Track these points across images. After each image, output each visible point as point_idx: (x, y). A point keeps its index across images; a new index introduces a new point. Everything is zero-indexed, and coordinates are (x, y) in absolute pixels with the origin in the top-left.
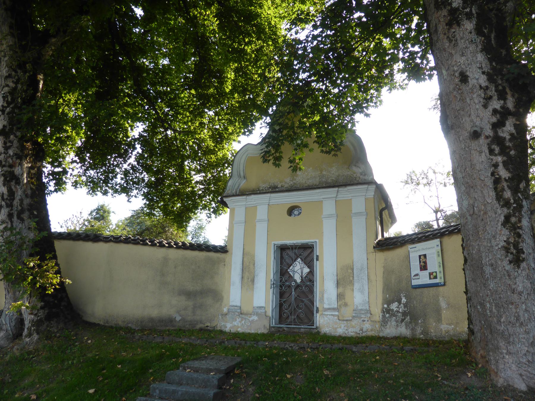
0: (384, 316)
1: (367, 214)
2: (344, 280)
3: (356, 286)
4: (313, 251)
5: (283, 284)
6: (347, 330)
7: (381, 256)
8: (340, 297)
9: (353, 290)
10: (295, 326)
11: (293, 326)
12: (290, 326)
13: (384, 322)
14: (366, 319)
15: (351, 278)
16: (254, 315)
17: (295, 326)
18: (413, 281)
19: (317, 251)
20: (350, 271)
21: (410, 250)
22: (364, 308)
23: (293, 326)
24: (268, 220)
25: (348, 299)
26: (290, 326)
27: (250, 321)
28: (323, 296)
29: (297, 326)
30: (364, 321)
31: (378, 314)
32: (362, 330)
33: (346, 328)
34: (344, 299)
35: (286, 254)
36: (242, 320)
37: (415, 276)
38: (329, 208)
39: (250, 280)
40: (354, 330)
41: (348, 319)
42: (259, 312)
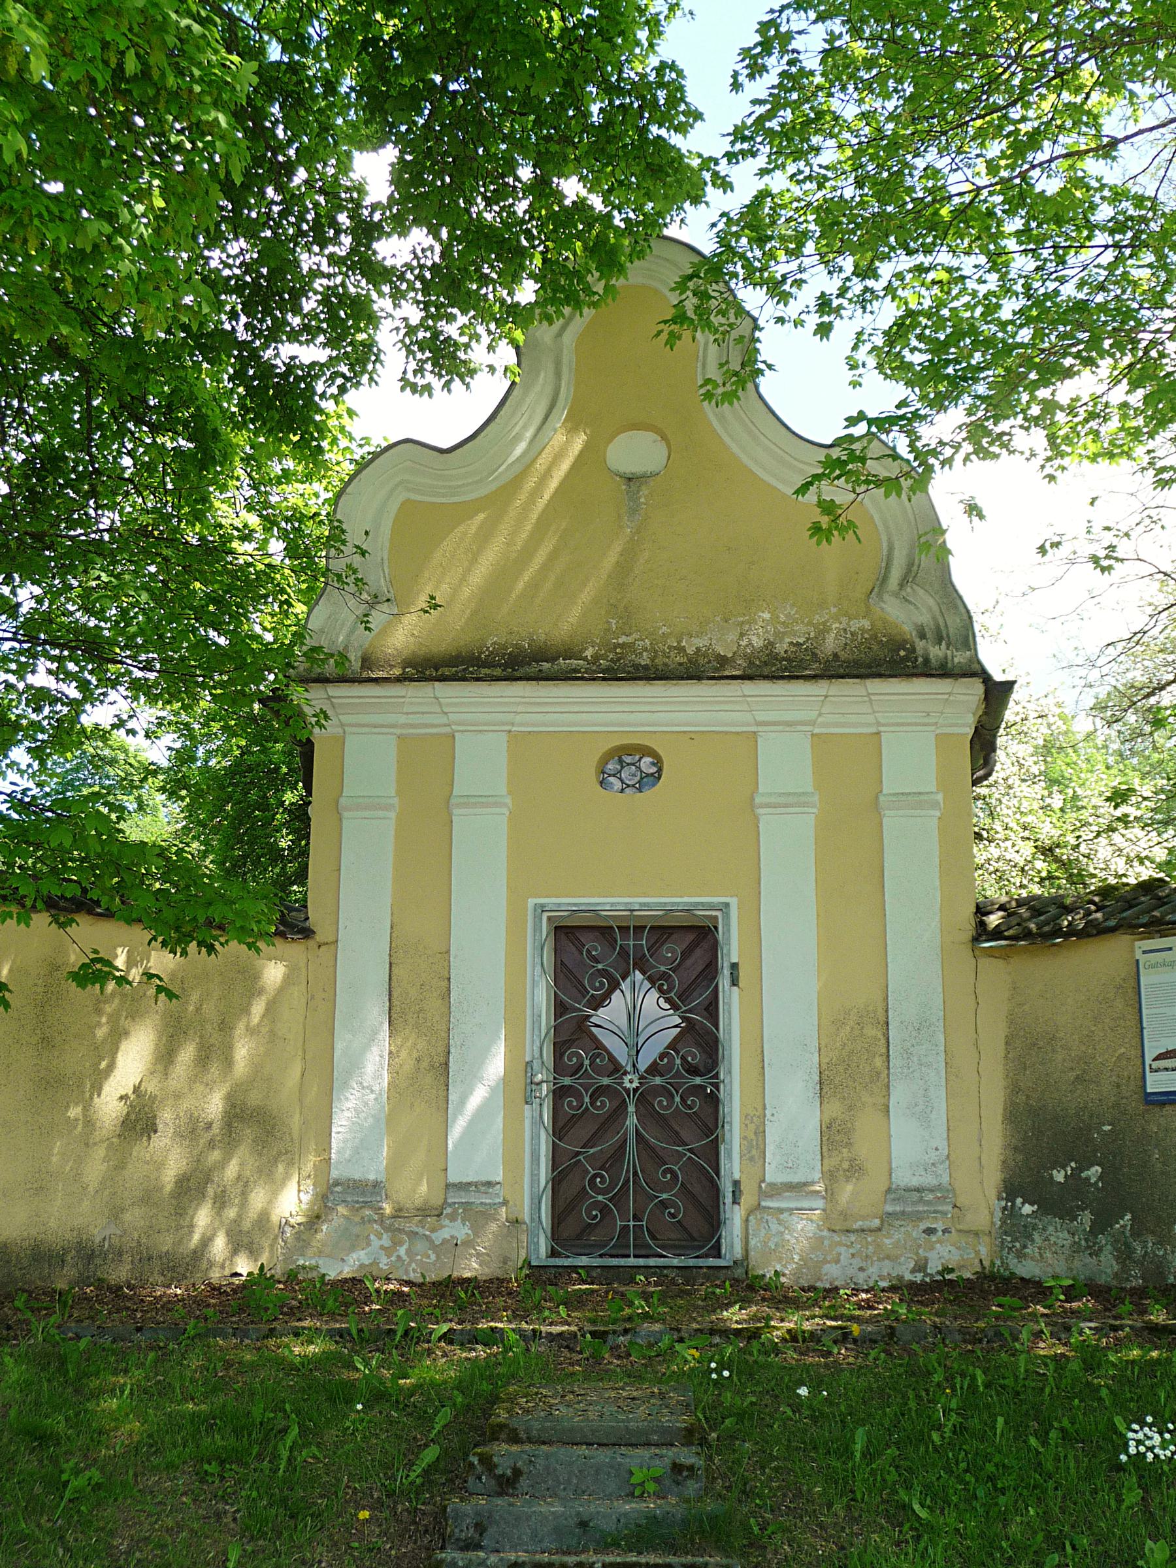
0: (1010, 1213)
1: (752, 805)
2: (854, 1071)
3: (899, 1095)
4: (715, 945)
5: (578, 1087)
6: (861, 1269)
7: (997, 974)
8: (833, 1136)
9: (887, 1110)
10: (641, 1262)
11: (632, 1261)
12: (622, 1262)
13: (1014, 1230)
14: (939, 1226)
15: (879, 1062)
16: (453, 1218)
17: (641, 1262)
18: (1149, 1076)
19: (733, 949)
20: (872, 1032)
21: (1142, 959)
22: (929, 1180)
23: (632, 1261)
24: (876, 807)
25: (863, 1149)
26: (622, 1262)
27: (434, 1247)
28: (761, 1133)
29: (652, 1262)
30: (930, 1231)
31: (982, 1200)
32: (921, 1267)
33: (857, 1263)
34: (849, 1145)
35: (587, 954)
36: (396, 1244)
37: (1158, 1058)
38: (785, 764)
39: (425, 1064)
40: (887, 1268)
41: (867, 1224)
42: (462, 1200)
